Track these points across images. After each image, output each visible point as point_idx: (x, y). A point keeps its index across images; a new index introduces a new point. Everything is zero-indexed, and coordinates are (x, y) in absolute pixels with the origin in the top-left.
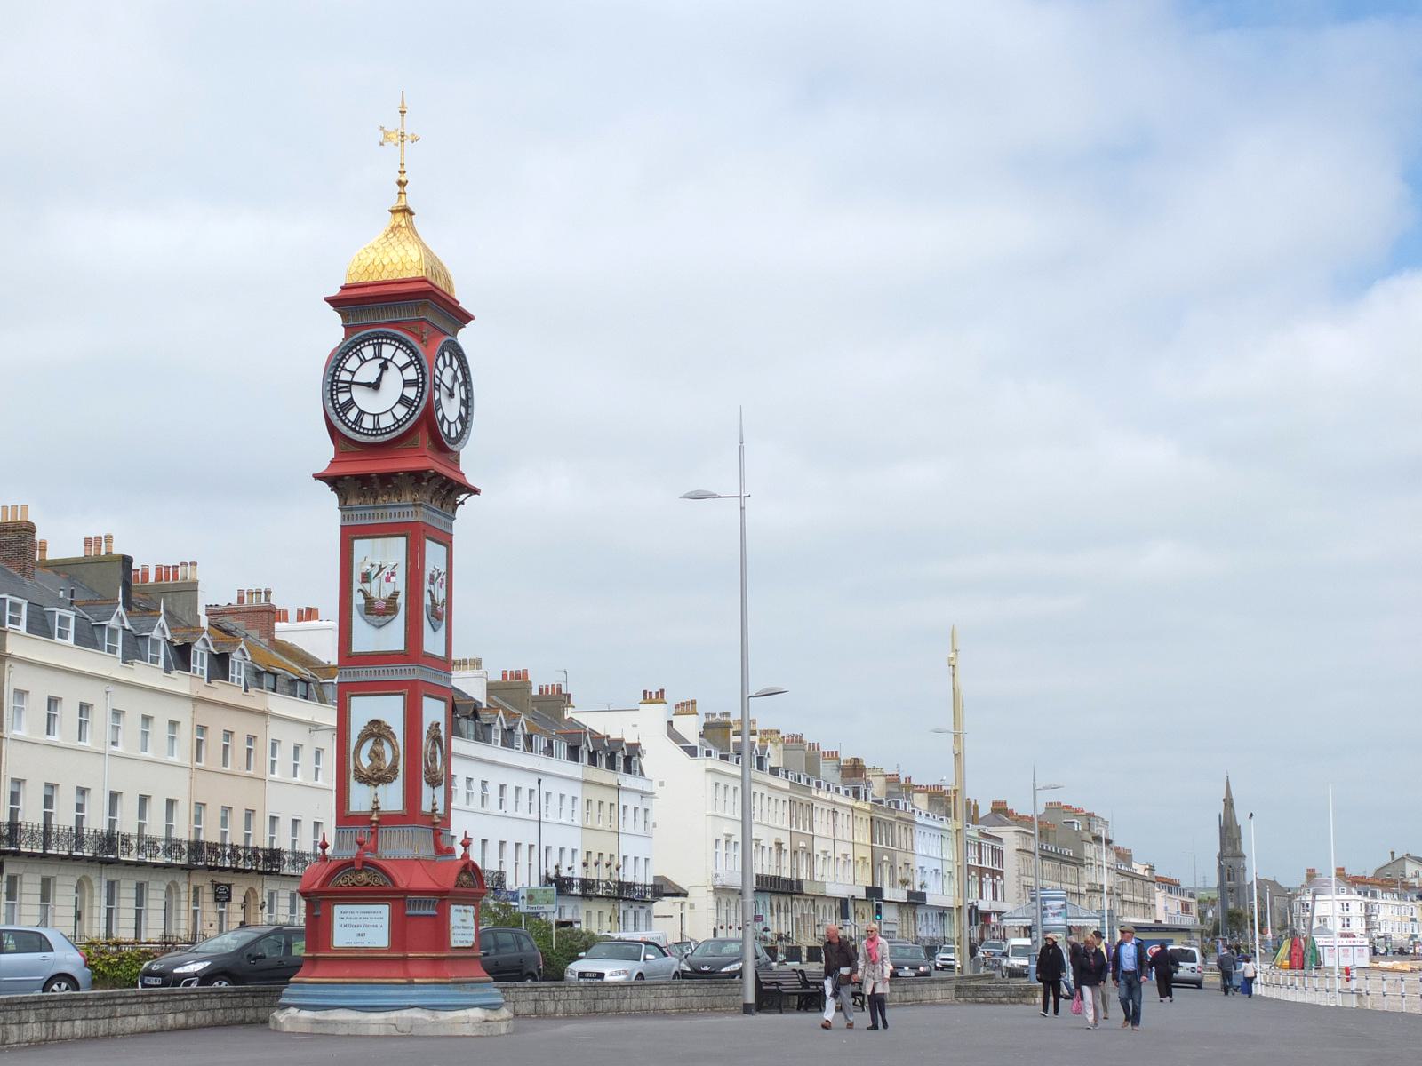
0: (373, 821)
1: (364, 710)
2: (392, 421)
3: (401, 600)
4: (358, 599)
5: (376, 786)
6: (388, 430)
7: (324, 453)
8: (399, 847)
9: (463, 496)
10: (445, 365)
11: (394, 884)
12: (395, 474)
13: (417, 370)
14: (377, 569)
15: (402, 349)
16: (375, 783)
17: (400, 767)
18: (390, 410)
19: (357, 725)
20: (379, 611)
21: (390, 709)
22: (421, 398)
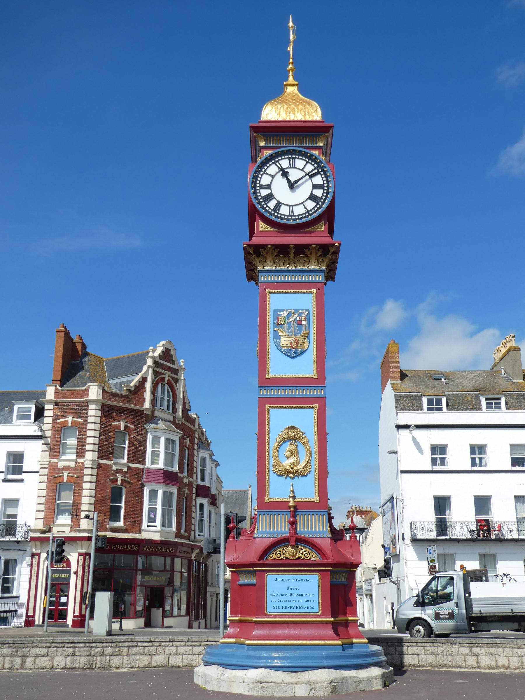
0: (290, 507)
2: (304, 211)
5: (293, 478)
8: (313, 527)
12: (308, 246)
13: (322, 178)
15: (311, 163)
16: (292, 476)
18: (302, 203)
22: (326, 197)
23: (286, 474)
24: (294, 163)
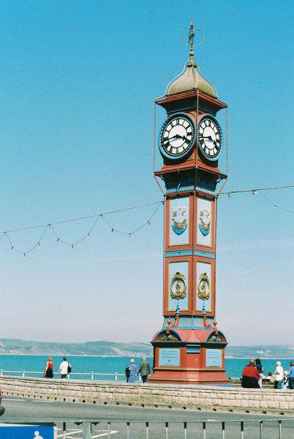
1: (175, 268)
4: (171, 223)
6: (181, 153)
7: (160, 165)
9: (219, 180)
10: (206, 126)
11: (179, 339)
17: (187, 290)
19: (172, 275)
20: (178, 229)
21: (183, 268)
23: (174, 297)
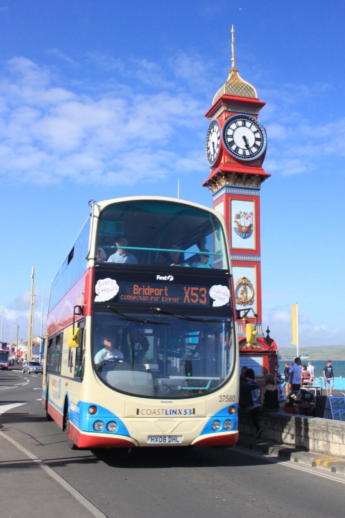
3: (254, 228)
12: (254, 175)
14: (243, 214)
24: (245, 124)
